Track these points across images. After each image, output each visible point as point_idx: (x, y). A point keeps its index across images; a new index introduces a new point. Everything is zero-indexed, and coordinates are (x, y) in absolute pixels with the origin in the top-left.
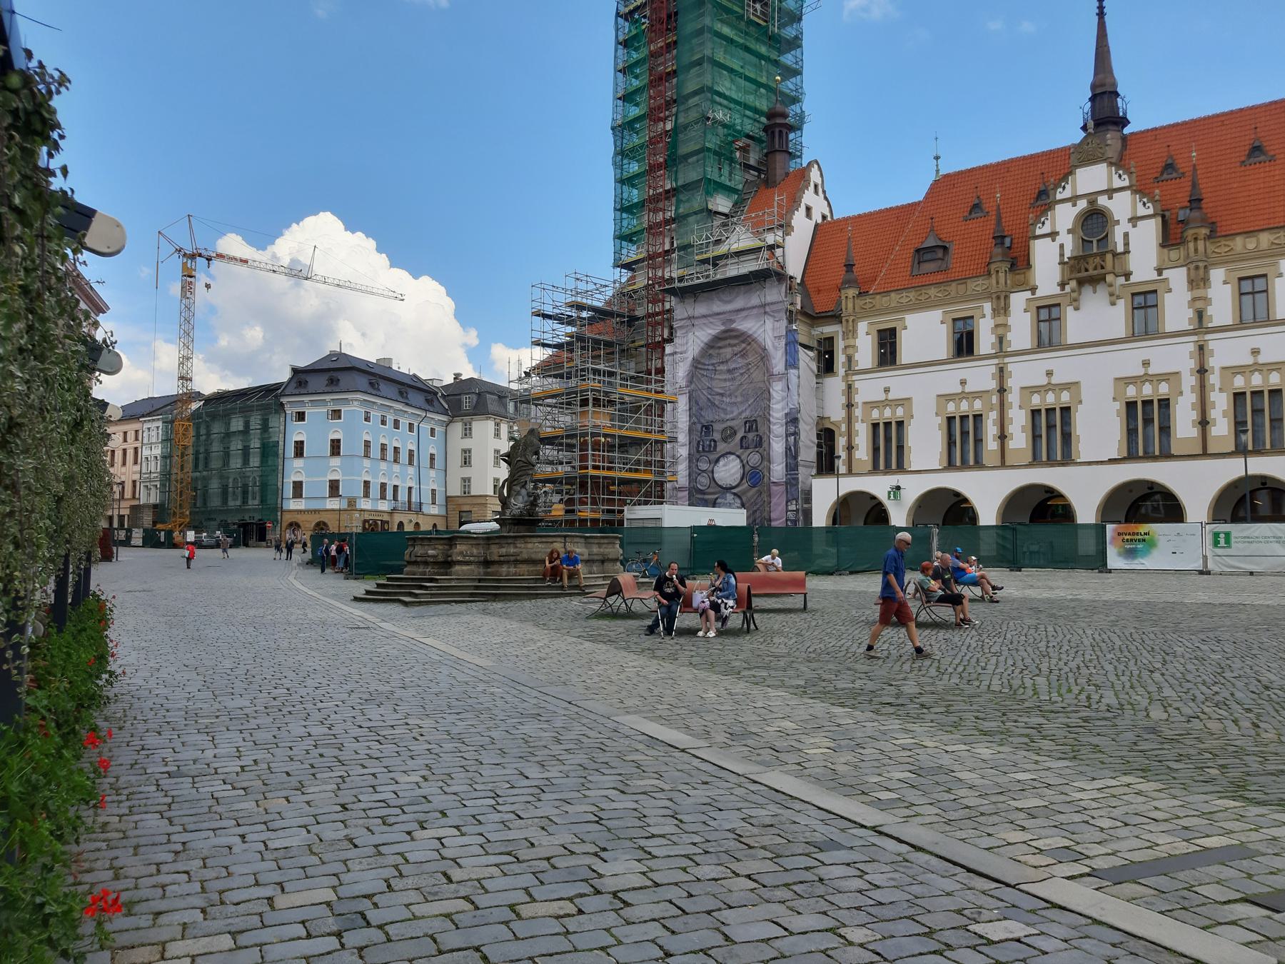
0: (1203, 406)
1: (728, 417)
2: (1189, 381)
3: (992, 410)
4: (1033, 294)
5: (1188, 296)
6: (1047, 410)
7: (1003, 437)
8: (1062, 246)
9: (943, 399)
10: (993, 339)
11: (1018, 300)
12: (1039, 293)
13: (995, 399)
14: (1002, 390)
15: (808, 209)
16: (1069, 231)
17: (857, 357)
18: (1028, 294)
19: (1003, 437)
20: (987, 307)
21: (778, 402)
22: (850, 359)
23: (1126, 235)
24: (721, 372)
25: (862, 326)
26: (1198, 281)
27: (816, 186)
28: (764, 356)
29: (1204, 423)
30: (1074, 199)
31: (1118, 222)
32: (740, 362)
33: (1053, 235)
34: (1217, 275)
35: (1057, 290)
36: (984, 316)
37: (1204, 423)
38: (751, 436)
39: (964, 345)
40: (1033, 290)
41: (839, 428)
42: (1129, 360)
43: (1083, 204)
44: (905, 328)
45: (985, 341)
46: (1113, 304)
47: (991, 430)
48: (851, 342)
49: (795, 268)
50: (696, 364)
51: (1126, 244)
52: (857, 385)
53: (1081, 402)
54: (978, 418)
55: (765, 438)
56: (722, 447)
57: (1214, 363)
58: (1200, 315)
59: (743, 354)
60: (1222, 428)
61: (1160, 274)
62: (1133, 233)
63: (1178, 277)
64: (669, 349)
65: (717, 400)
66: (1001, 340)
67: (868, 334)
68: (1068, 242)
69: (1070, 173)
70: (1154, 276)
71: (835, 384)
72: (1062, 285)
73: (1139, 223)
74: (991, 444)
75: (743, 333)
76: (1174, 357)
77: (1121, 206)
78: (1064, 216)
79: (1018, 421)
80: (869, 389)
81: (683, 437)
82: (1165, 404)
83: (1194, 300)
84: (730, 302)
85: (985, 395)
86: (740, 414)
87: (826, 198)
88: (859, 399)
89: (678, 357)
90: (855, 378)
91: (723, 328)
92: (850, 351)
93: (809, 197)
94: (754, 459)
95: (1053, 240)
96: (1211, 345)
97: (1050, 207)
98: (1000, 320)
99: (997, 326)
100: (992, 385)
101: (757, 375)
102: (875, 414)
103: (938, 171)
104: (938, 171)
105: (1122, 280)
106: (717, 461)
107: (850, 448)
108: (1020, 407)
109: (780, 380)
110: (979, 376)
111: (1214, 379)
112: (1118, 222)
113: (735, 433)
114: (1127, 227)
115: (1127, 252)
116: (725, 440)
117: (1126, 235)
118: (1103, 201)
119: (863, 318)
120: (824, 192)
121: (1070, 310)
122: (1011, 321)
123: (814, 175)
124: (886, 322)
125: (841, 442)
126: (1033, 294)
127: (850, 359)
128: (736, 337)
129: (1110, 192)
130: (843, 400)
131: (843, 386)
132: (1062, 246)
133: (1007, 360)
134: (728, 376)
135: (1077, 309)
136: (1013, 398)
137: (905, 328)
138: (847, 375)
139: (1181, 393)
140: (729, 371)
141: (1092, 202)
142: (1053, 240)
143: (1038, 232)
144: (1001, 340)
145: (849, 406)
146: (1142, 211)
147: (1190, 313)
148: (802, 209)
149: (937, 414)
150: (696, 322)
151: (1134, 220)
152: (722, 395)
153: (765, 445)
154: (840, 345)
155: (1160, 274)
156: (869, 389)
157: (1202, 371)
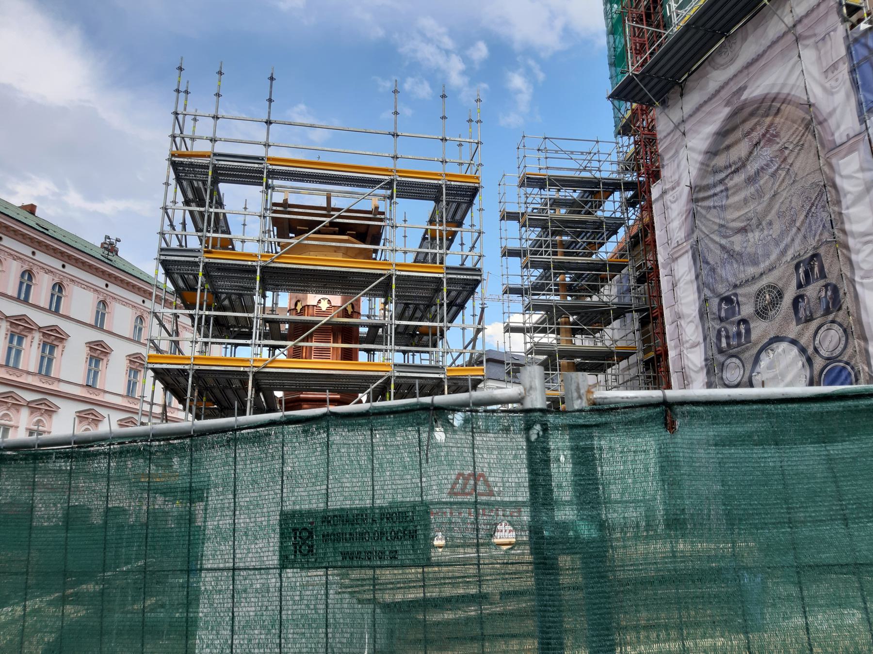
1: (763, 266)
21: (855, 203)
24: (738, 189)
28: (811, 121)
32: (767, 152)
38: (812, 291)
50: (698, 193)
55: (844, 287)
56: (760, 329)
59: (769, 137)
64: (655, 191)
65: (737, 242)
75: (764, 99)
81: (692, 331)
84: (732, 61)
86: (783, 253)
89: (668, 197)
91: (726, 111)
94: (830, 340)
101: (803, 164)
106: (757, 360)
109: (850, 151)
113: (780, 294)
116: (762, 313)
128: (752, 114)
134: (752, 189)
140: (751, 180)
150: (687, 126)
152: (743, 230)
153: (848, 302)
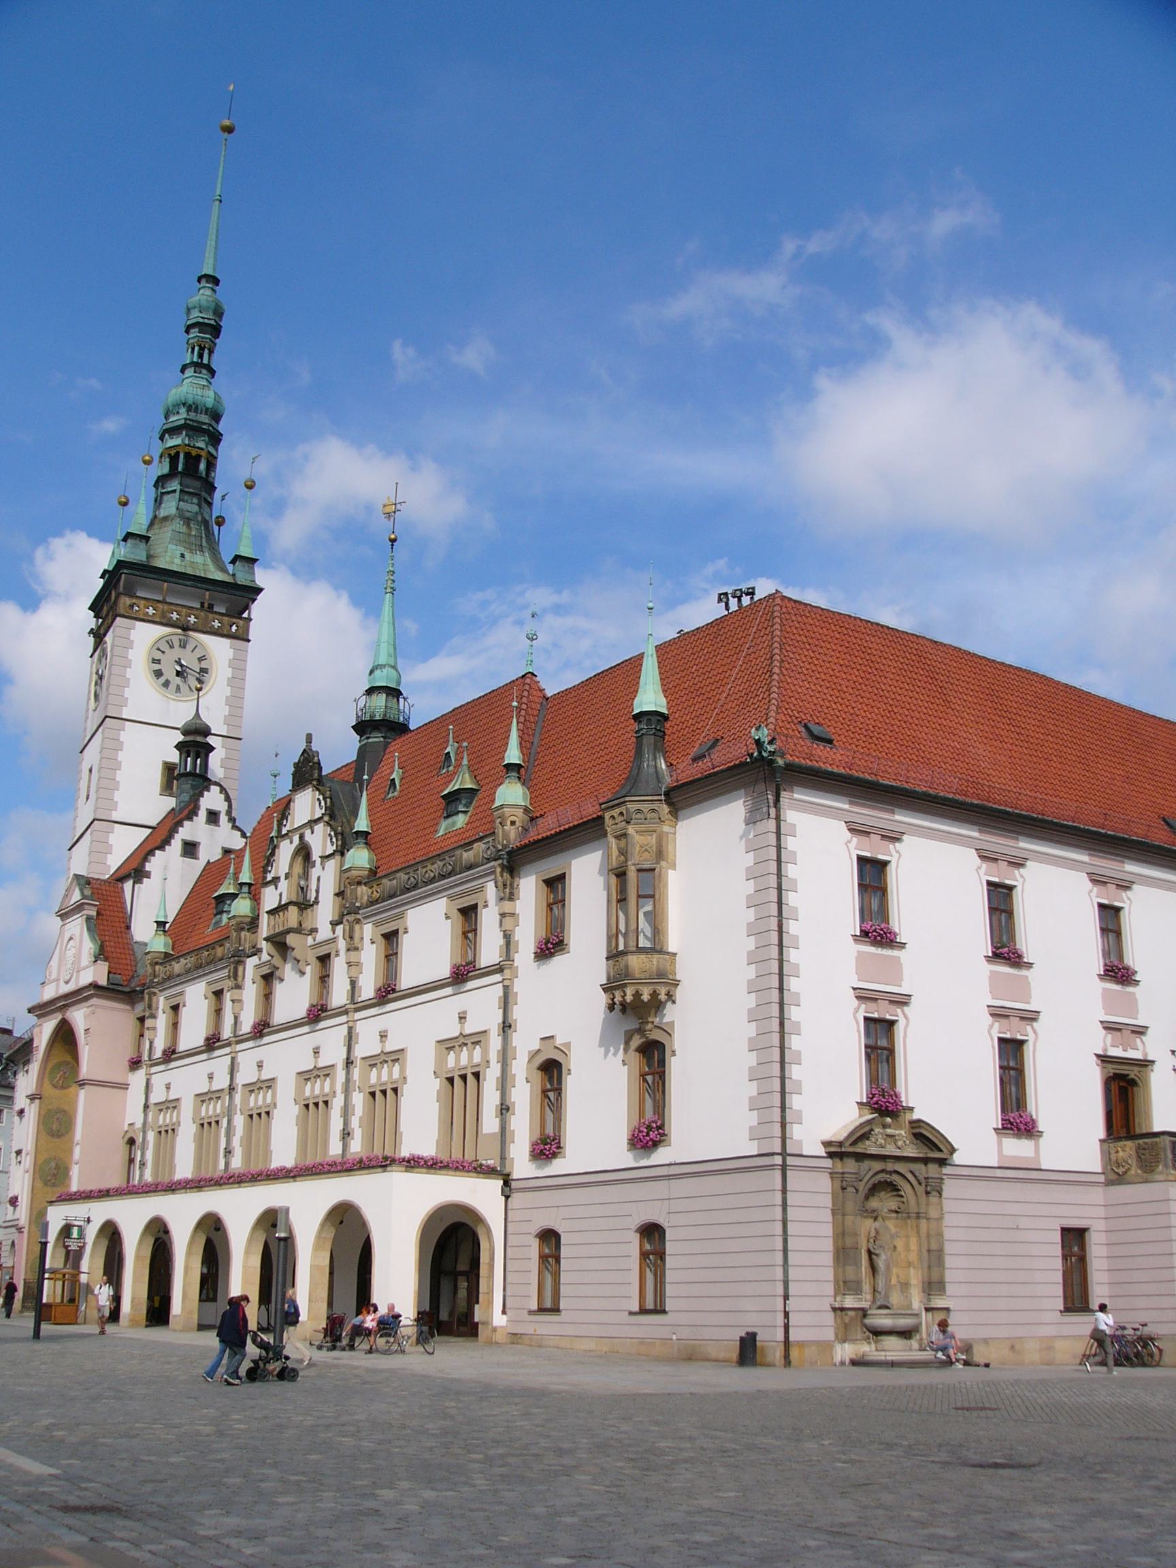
0: (346, 1112)
14: (232, 1089)
15: (190, 849)
19: (228, 1152)
23: (319, 879)
27: (213, 817)
29: (346, 1134)
49: (143, 930)
51: (317, 891)
57: (360, 1051)
71: (137, 1079)
87: (235, 827)
88: (154, 1099)
93: (186, 832)
96: (360, 1027)
105: (310, 940)
107: (143, 1164)
115: (316, 902)
117: (319, 879)
120: (232, 820)
123: (212, 800)
127: (151, 1043)
136: (238, 1098)
141: (302, 837)
145: (146, 1107)
148: (176, 844)
151: (325, 858)
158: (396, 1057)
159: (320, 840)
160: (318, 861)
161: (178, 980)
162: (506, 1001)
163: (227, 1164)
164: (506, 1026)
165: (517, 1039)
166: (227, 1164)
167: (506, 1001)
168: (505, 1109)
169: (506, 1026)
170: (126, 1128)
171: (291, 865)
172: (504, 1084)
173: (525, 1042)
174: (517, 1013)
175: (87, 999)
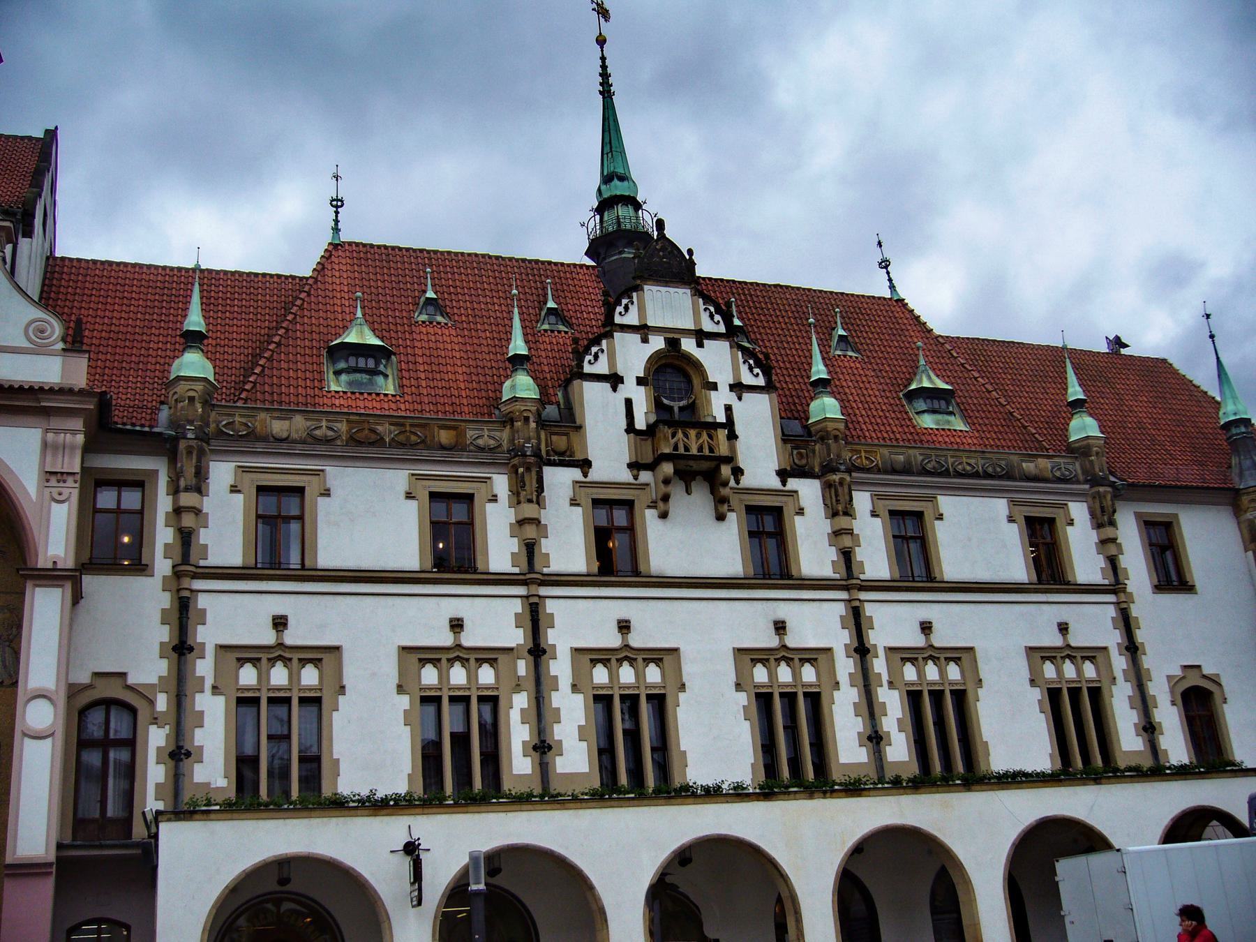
0: (870, 708)
2: (845, 666)
3: (518, 688)
4: (585, 475)
5: (826, 526)
6: (623, 697)
7: (543, 748)
8: (629, 403)
9: (414, 658)
10: (514, 545)
11: (559, 480)
12: (595, 474)
13: (522, 667)
14: (538, 652)
16: (640, 381)
17: (204, 537)
18: (576, 474)
19: (543, 748)
20: (501, 483)
22: (186, 538)
23: (728, 409)
25: (221, 472)
26: (839, 507)
29: (875, 739)
30: (644, 331)
31: (714, 386)
33: (615, 380)
34: (862, 501)
35: (625, 476)
36: (494, 499)
37: (875, 739)
39: (453, 555)
40: (585, 465)
41: (152, 703)
42: (748, 622)
43: (658, 343)
44: (327, 493)
45: (500, 551)
46: (721, 517)
47: (518, 734)
48: (187, 499)
52: (203, 601)
53: (683, 687)
54: (491, 701)
58: (847, 556)
60: (899, 750)
61: (784, 483)
62: (738, 407)
63: (809, 491)
66: (530, 548)
67: (234, 489)
68: (642, 399)
69: (638, 288)
70: (775, 483)
72: (635, 466)
73: (745, 396)
74: (519, 764)
76: (817, 623)
77: (717, 360)
78: (632, 355)
79: (572, 714)
80: (233, 617)
82: (814, 699)
83: (837, 533)
85: (502, 658)
88: (208, 635)
90: (198, 584)
92: (188, 521)
95: (615, 389)
97: (609, 328)
98: (529, 510)
99: (521, 522)
100: (516, 637)
102: (248, 676)
103: (336, 230)
104: (336, 230)
107: (179, 754)
108: (575, 688)
110: (494, 621)
111: (879, 665)
112: (714, 386)
114: (731, 398)
117: (728, 409)
118: (688, 345)
119: (224, 453)
121: (650, 515)
122: (546, 517)
124: (282, 468)
125: (157, 738)
126: (585, 475)
127: (186, 538)
129: (701, 336)
130: (164, 634)
131: (165, 600)
132: (629, 403)
133: (544, 591)
135: (664, 515)
136: (560, 668)
137: (327, 493)
138: (177, 574)
139: (837, 685)
141: (673, 344)
142: (615, 389)
143: (587, 369)
144: (530, 548)
146: (747, 379)
147: (832, 554)
149: (401, 689)
154: (164, 503)
155: (784, 483)
156: (233, 617)
157: (862, 651)
158: (962, 655)
159: (717, 360)
160: (724, 388)
161: (298, 449)
162: (1126, 622)
163: (544, 769)
164: (1132, 648)
165: (1147, 662)
166: (544, 769)
167: (1126, 622)
168: (1149, 729)
169: (1132, 648)
170: (84, 678)
171: (647, 369)
172: (1144, 703)
173: (1162, 668)
174: (1140, 636)
175: (47, 412)
